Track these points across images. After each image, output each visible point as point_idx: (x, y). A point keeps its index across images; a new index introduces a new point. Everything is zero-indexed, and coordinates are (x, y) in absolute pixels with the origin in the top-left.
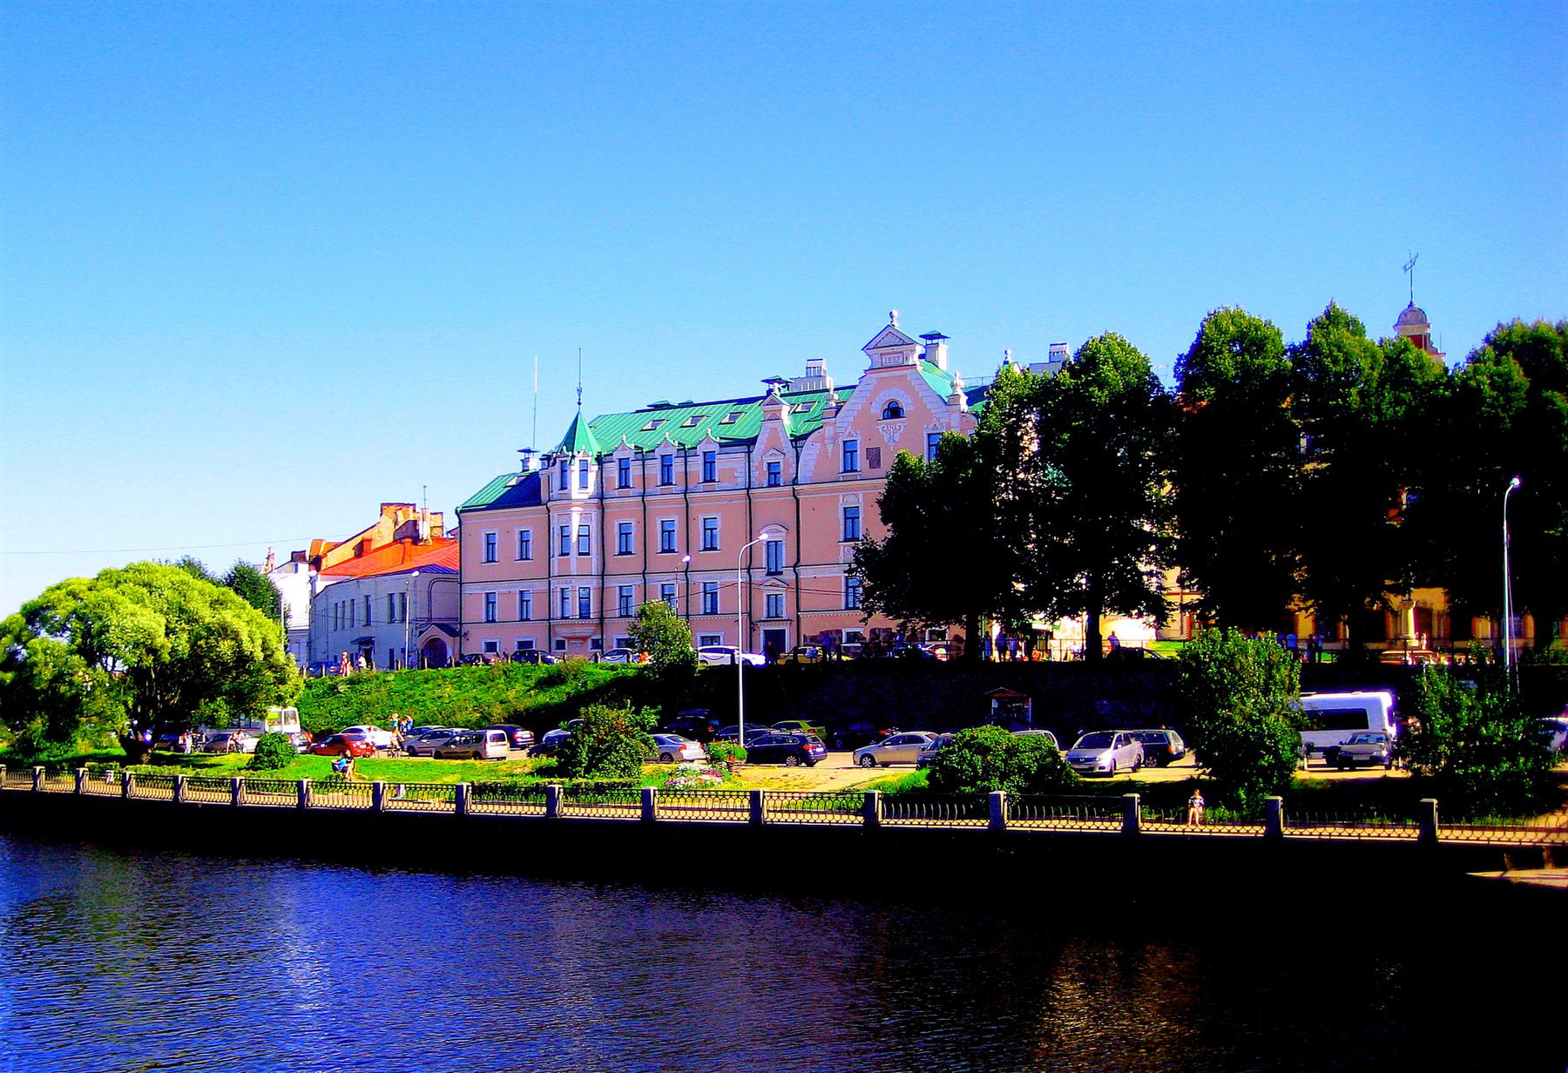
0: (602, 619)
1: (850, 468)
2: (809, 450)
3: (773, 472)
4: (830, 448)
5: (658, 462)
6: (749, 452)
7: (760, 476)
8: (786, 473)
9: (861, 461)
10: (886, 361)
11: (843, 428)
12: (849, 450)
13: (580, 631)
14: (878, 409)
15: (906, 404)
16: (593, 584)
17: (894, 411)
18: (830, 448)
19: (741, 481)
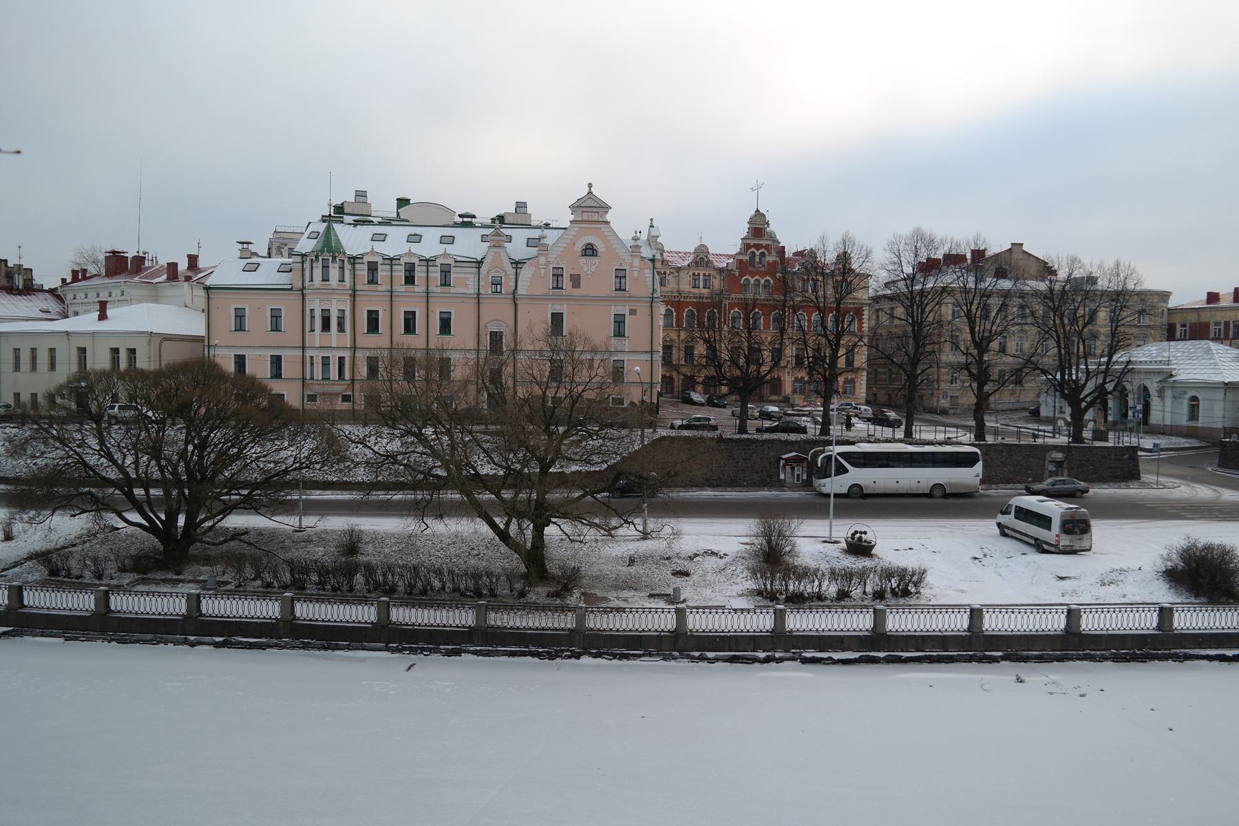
0: (353, 380)
1: (557, 287)
2: (526, 273)
3: (497, 283)
4: (543, 271)
5: (366, 267)
6: (479, 268)
7: (487, 289)
8: (508, 286)
9: (566, 282)
10: (585, 217)
11: (554, 258)
12: (558, 276)
13: (337, 389)
14: (579, 247)
15: (601, 248)
16: (347, 355)
17: (590, 251)
18: (543, 271)
19: (472, 290)
